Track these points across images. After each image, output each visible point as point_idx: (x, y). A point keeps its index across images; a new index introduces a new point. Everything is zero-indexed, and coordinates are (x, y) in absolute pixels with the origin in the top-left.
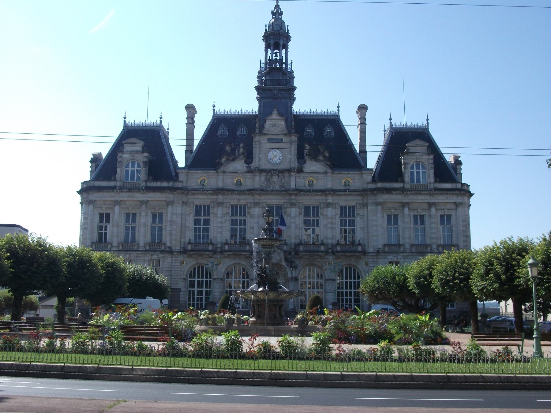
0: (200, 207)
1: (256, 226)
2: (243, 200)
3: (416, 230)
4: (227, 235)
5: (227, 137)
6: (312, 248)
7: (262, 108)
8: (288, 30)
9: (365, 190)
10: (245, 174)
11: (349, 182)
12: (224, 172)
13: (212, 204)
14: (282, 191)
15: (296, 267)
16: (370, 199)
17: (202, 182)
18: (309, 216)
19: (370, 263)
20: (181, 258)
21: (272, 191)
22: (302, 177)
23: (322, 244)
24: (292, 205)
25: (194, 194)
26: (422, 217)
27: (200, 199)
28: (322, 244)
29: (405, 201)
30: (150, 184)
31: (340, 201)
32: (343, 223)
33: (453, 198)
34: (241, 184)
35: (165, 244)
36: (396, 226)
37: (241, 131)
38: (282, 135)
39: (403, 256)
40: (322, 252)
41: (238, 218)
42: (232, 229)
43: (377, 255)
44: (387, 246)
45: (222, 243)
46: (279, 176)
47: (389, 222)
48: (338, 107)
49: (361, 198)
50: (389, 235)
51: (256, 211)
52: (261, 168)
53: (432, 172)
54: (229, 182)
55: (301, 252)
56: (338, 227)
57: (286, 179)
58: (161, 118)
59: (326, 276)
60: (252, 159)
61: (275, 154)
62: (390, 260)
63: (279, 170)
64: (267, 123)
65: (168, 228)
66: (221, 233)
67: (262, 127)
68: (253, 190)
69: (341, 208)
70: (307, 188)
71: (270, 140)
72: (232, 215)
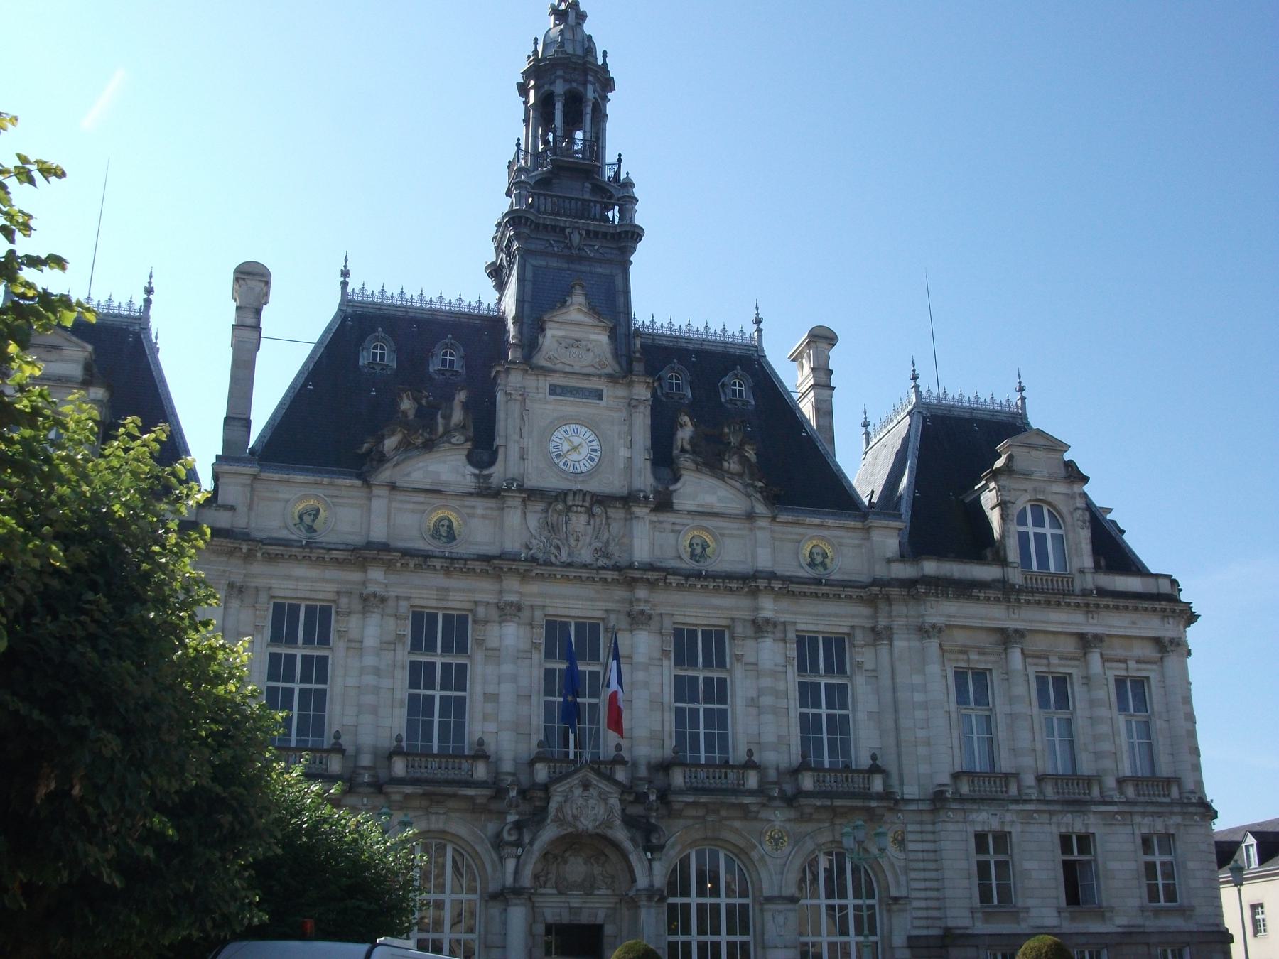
0: (294, 609)
1: (507, 689)
2: (462, 593)
4: (396, 722)
5: (381, 384)
7: (529, 287)
8: (605, 63)
9: (876, 582)
10: (470, 502)
11: (825, 556)
12: (393, 487)
13: (344, 601)
14: (603, 568)
15: (661, 848)
16: (901, 614)
17: (307, 519)
19: (910, 837)
21: (570, 565)
22: (668, 526)
23: (750, 765)
24: (637, 619)
25: (271, 558)
26: (1062, 682)
27: (298, 579)
28: (750, 765)
29: (1012, 625)
31: (799, 619)
32: (808, 694)
33: (1153, 626)
34: (451, 536)
36: (982, 711)
37: (447, 358)
38: (600, 376)
39: (1017, 812)
40: (751, 793)
41: (439, 661)
42: (413, 700)
43: (934, 811)
44: (965, 779)
45: (375, 752)
46: (591, 515)
47: (962, 699)
48: (758, 321)
49: (865, 611)
51: (511, 635)
52: (528, 484)
53: (1085, 535)
55: (681, 792)
56: (795, 710)
57: (616, 527)
58: (149, 291)
59: (765, 885)
61: (575, 437)
62: (979, 829)
63: (593, 495)
64: (549, 333)
66: (374, 710)
67: (530, 344)
68: (499, 557)
69: (801, 641)
70: (688, 564)
71: (554, 390)
72: (416, 646)
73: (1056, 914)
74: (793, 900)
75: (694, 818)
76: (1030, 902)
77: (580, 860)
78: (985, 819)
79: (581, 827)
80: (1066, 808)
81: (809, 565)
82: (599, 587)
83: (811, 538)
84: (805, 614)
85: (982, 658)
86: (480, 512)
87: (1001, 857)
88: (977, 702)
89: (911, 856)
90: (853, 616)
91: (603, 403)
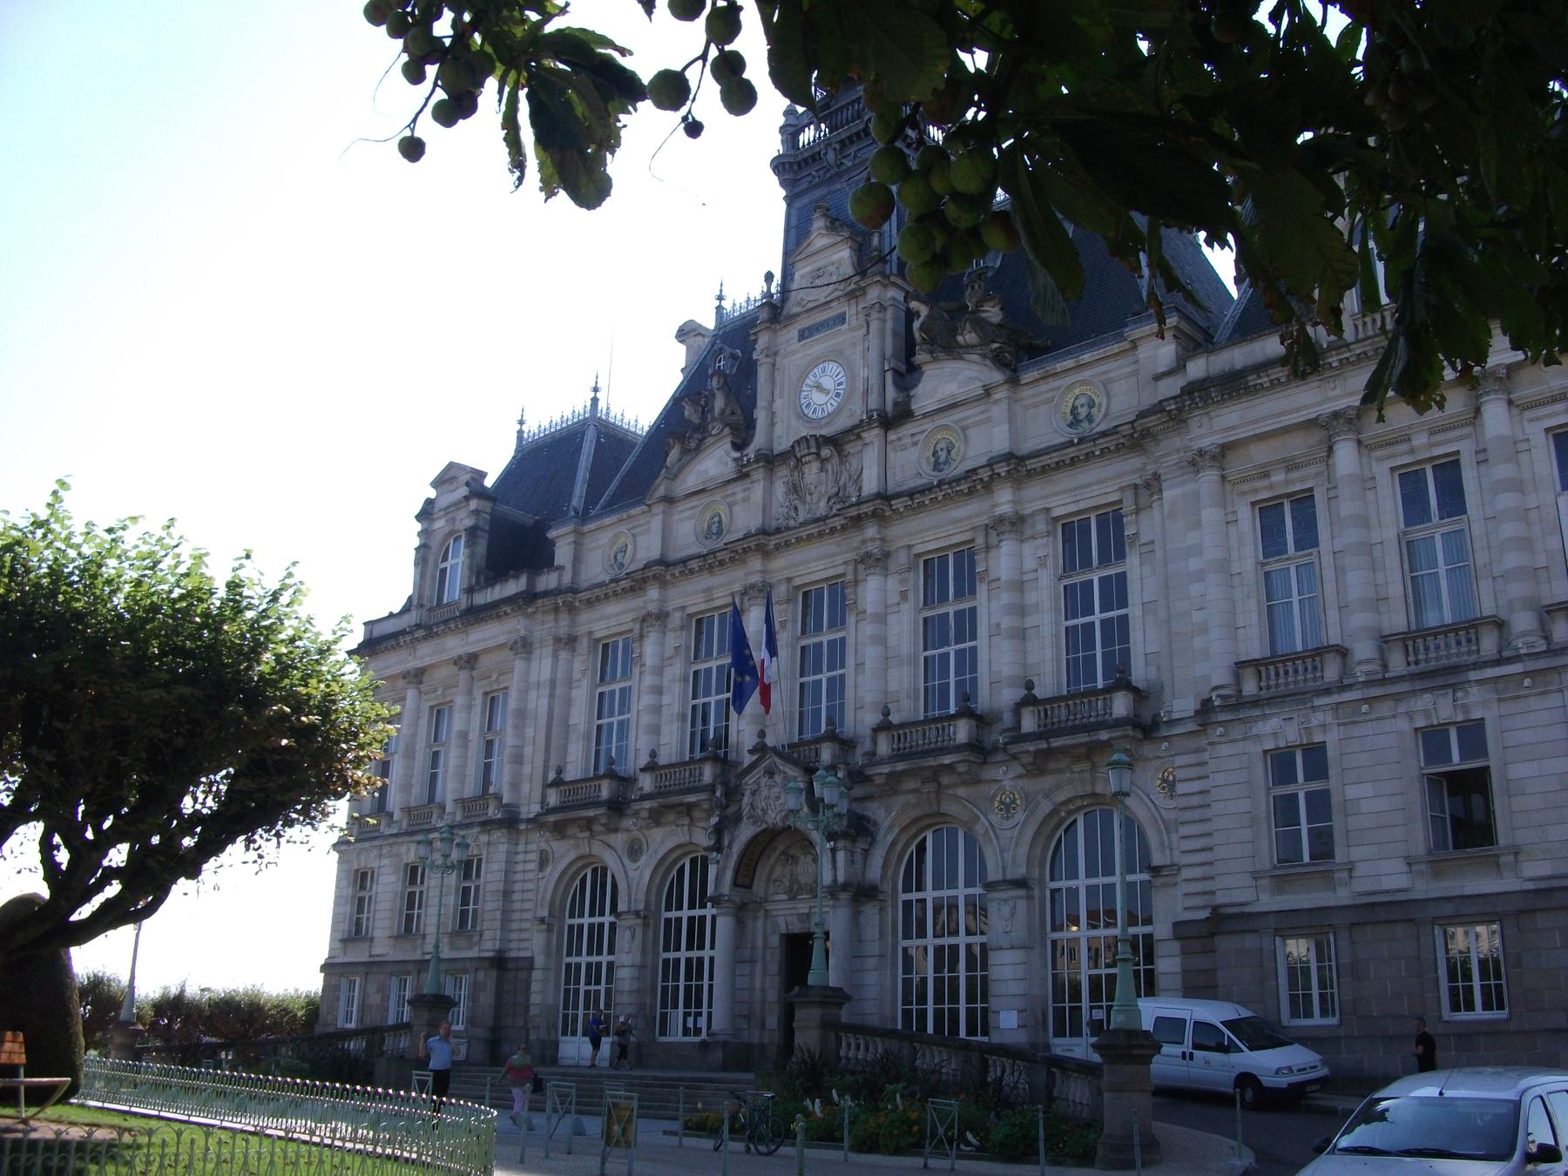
3: (1411, 552)
6: (916, 739)
7: (793, 232)
10: (731, 489)
11: (1091, 404)
12: (669, 500)
16: (1170, 449)
17: (620, 556)
18: (943, 598)
20: (538, 842)
22: (908, 441)
26: (1449, 471)
30: (482, 598)
35: (498, 797)
46: (823, 461)
50: (1273, 616)
54: (687, 531)
59: (990, 867)
60: (750, 424)
64: (797, 276)
65: (510, 739)
70: (929, 476)
71: (802, 336)
73: (1404, 868)
74: (1021, 883)
75: (913, 791)
76: (1356, 853)
77: (809, 858)
78: (1281, 728)
79: (770, 821)
80: (1418, 685)
81: (1071, 425)
82: (837, 538)
83: (1071, 387)
84: (1058, 493)
85: (1294, 475)
86: (739, 496)
87: (1316, 786)
88: (1299, 546)
89: (1183, 802)
90: (1120, 475)
91: (845, 327)
